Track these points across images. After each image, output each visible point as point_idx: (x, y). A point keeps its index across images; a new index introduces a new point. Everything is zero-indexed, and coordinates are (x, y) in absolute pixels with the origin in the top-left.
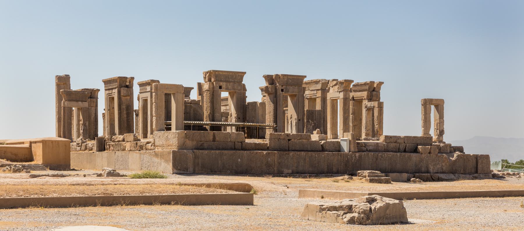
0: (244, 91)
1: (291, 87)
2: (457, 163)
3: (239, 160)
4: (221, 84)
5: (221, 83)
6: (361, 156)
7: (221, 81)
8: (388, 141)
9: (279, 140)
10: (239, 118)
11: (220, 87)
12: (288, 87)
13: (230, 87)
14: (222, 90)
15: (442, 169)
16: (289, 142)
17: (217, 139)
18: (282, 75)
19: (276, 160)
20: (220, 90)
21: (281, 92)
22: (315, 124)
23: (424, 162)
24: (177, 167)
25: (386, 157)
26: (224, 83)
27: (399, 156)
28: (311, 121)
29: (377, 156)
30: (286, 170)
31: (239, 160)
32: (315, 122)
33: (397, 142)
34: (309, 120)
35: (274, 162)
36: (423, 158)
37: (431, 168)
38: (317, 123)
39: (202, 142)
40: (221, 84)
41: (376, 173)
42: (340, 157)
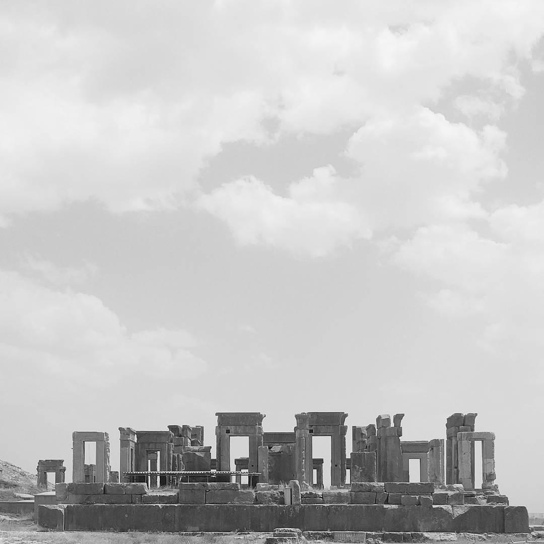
1: (323, 427)
2: (468, 519)
3: (126, 516)
5: (228, 427)
6: (304, 509)
8: (357, 490)
9: (192, 492)
11: (228, 432)
12: (319, 427)
13: (240, 430)
14: (229, 434)
15: (441, 526)
16: (207, 493)
17: (108, 491)
19: (176, 516)
20: (227, 434)
22: (363, 469)
23: (408, 517)
24: (44, 524)
25: (343, 511)
26: (233, 427)
27: (364, 509)
29: (329, 509)
30: (191, 527)
31: (126, 516)
32: (364, 467)
33: (372, 491)
35: (174, 518)
36: (406, 511)
37: (420, 526)
38: (366, 469)
39: (88, 496)
41: (291, 531)
42: (270, 510)
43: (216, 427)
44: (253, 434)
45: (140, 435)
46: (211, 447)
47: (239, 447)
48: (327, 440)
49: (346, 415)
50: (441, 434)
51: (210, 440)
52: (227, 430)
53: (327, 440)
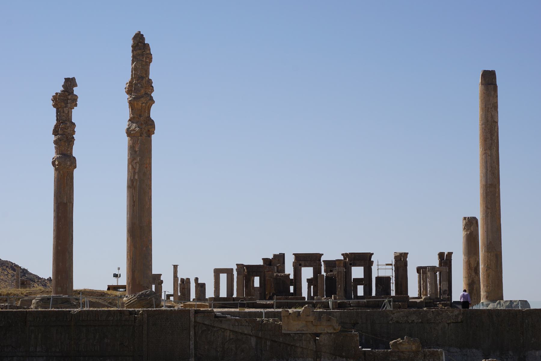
0: (320, 267)
4: (301, 262)
5: (301, 262)
7: (300, 260)
10: (315, 286)
14: (301, 266)
18: (349, 253)
20: (300, 266)
21: (349, 266)
26: (303, 262)
28: (379, 286)
32: (383, 286)
34: (378, 285)
40: (301, 262)
43: (293, 262)
44: (315, 266)
45: (248, 267)
46: (290, 274)
47: (307, 273)
48: (361, 269)
49: (373, 254)
50: (435, 262)
51: (289, 270)
52: (299, 264)
53: (361, 269)
